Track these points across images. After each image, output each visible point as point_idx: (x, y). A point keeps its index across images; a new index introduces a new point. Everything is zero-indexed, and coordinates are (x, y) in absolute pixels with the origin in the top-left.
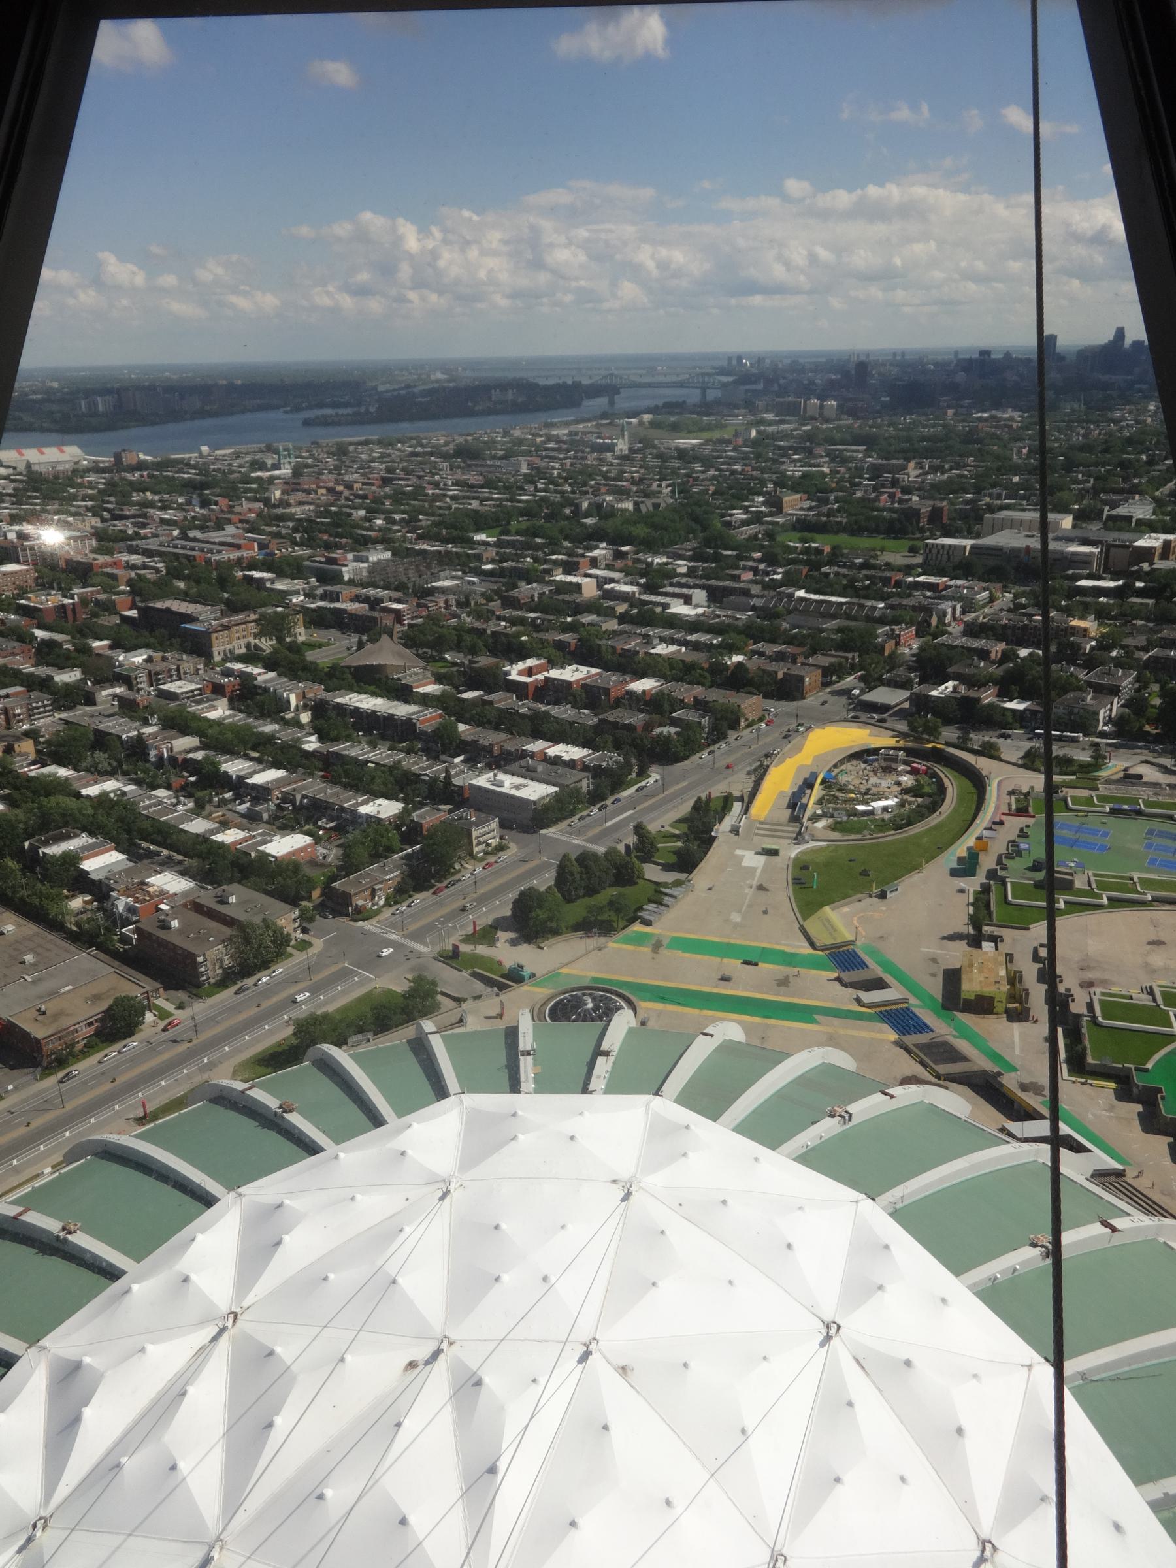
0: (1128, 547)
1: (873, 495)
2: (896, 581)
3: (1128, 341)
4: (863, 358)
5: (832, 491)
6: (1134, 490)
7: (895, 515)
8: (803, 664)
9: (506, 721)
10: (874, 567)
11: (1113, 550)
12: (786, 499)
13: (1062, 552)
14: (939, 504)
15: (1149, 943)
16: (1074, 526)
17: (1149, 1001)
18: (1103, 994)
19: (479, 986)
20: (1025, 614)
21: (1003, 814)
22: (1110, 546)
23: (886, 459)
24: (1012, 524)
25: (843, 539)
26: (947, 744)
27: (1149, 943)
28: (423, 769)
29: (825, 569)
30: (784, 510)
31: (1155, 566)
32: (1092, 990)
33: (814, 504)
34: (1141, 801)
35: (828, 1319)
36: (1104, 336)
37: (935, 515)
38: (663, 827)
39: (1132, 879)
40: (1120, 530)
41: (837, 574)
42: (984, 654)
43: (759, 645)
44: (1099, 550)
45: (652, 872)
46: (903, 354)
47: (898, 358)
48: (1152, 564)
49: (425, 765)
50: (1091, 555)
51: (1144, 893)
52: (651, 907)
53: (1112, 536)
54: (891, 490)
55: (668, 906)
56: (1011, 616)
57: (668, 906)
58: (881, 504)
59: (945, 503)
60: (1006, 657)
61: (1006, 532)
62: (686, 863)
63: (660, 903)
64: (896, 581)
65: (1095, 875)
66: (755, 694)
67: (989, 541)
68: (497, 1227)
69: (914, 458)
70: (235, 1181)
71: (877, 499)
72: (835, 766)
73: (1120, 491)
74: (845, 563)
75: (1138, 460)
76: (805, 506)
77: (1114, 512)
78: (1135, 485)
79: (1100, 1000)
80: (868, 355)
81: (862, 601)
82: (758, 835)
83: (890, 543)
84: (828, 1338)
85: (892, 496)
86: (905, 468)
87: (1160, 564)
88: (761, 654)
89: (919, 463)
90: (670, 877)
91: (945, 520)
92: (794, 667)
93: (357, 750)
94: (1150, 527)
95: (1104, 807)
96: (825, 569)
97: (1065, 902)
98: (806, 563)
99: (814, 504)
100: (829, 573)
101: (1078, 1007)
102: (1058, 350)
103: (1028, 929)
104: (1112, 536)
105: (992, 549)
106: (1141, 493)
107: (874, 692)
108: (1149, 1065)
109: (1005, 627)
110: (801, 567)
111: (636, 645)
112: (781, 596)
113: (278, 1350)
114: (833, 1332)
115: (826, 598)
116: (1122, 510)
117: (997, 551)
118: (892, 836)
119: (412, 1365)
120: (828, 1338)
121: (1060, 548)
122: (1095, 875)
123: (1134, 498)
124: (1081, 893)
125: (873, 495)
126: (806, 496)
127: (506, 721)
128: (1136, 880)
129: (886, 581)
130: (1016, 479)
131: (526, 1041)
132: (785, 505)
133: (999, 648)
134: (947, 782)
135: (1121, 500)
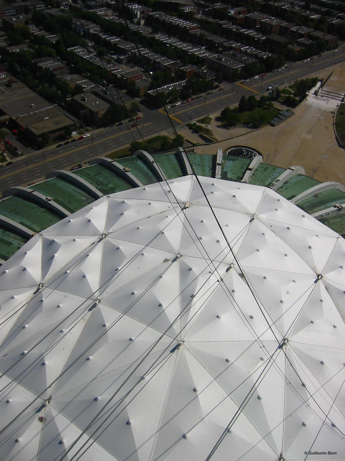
9: (227, 34)
19: (202, 141)
28: (189, 49)
35: (319, 273)
38: (286, 87)
45: (277, 105)
49: (190, 48)
52: (276, 119)
55: (282, 120)
57: (282, 120)
62: (292, 103)
63: (279, 118)
68: (202, 221)
70: (106, 192)
84: (318, 280)
90: (284, 108)
93: (160, 37)
111: (287, 7)
113: (120, 248)
114: (320, 277)
119: (166, 260)
120: (318, 280)
127: (227, 34)
131: (219, 160)
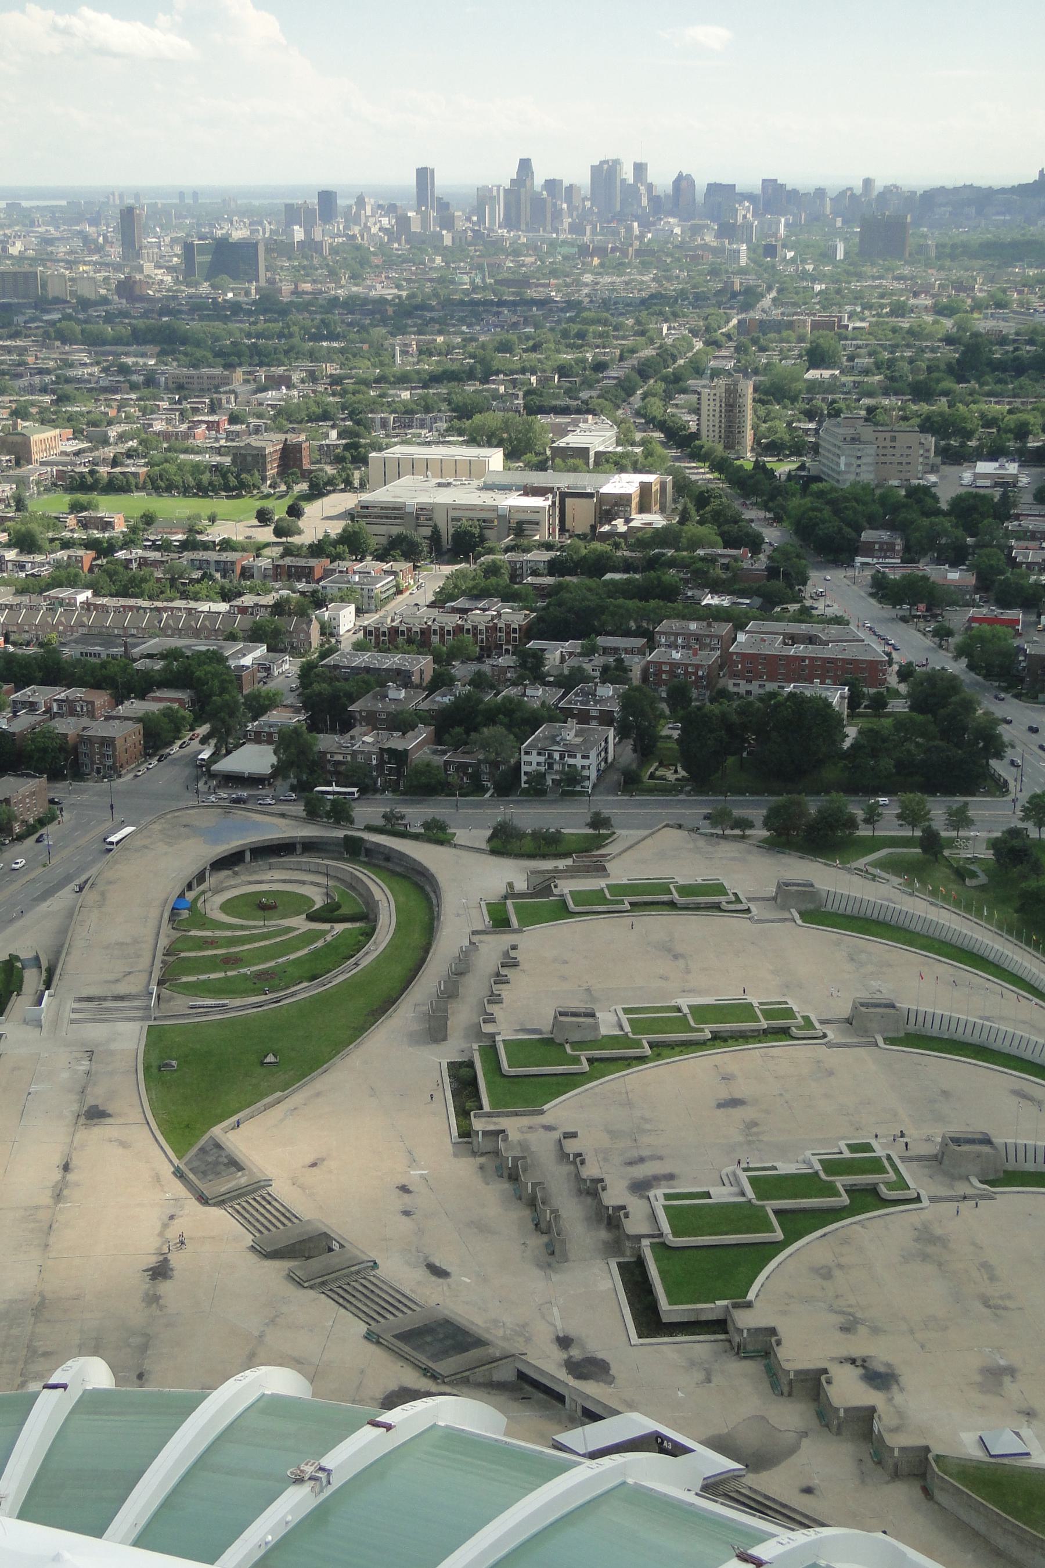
0: (590, 495)
1: (184, 427)
2: (243, 568)
3: (539, 180)
4: (130, 201)
5: (110, 423)
6: (586, 409)
7: (227, 460)
8: (108, 718)
10: (206, 546)
11: (568, 501)
12: (34, 438)
13: (495, 509)
14: (293, 438)
15: (720, 1106)
16: (506, 468)
17: (736, 1195)
18: (668, 1197)
20: (455, 610)
21: (475, 933)
22: (564, 496)
23: (195, 366)
24: (413, 466)
25: (139, 502)
26: (369, 828)
27: (722, 1105)
29: (121, 554)
30: (35, 457)
31: (632, 524)
32: (651, 1194)
33: (85, 445)
34: (671, 886)
36: (504, 175)
37: (289, 456)
39: (679, 1009)
40: (575, 469)
41: (143, 562)
42: (402, 677)
43: (28, 691)
44: (550, 502)
46: (195, 195)
47: (189, 201)
48: (628, 521)
50: (536, 510)
51: (702, 1030)
53: (563, 480)
54: (211, 418)
56: (435, 612)
58: (199, 442)
59: (302, 437)
60: (440, 682)
61: (406, 480)
64: (243, 568)
65: (626, 1011)
66: (36, 777)
67: (381, 495)
69: (240, 365)
71: (186, 435)
72: (190, 887)
73: (564, 411)
74: (154, 541)
75: (584, 360)
76: (69, 449)
77: (562, 443)
78: (585, 402)
79: (665, 1207)
80: (137, 196)
81: (192, 604)
82: (73, 1021)
83: (220, 504)
85: (212, 426)
86: (227, 381)
87: (639, 520)
88: (32, 706)
89: (249, 373)
91: (306, 466)
92: (94, 724)
94: (619, 464)
95: (622, 902)
96: (121, 554)
97: (588, 1060)
98: (90, 544)
99: (85, 445)
100: (129, 561)
101: (636, 1224)
102: (437, 192)
103: (542, 1112)
104: (563, 480)
105: (386, 508)
106: (593, 412)
107: (235, 754)
108: (751, 1296)
109: (426, 633)
110: (81, 552)
112: (54, 605)
115: (131, 602)
116: (573, 440)
117: (394, 513)
118: (304, 991)
121: (490, 502)
122: (626, 1011)
123: (586, 421)
124: (613, 1041)
125: (184, 427)
126: (69, 432)
128: (686, 1010)
129: (225, 568)
130: (406, 395)
132: (34, 449)
133: (422, 665)
134: (378, 894)
135: (568, 424)
